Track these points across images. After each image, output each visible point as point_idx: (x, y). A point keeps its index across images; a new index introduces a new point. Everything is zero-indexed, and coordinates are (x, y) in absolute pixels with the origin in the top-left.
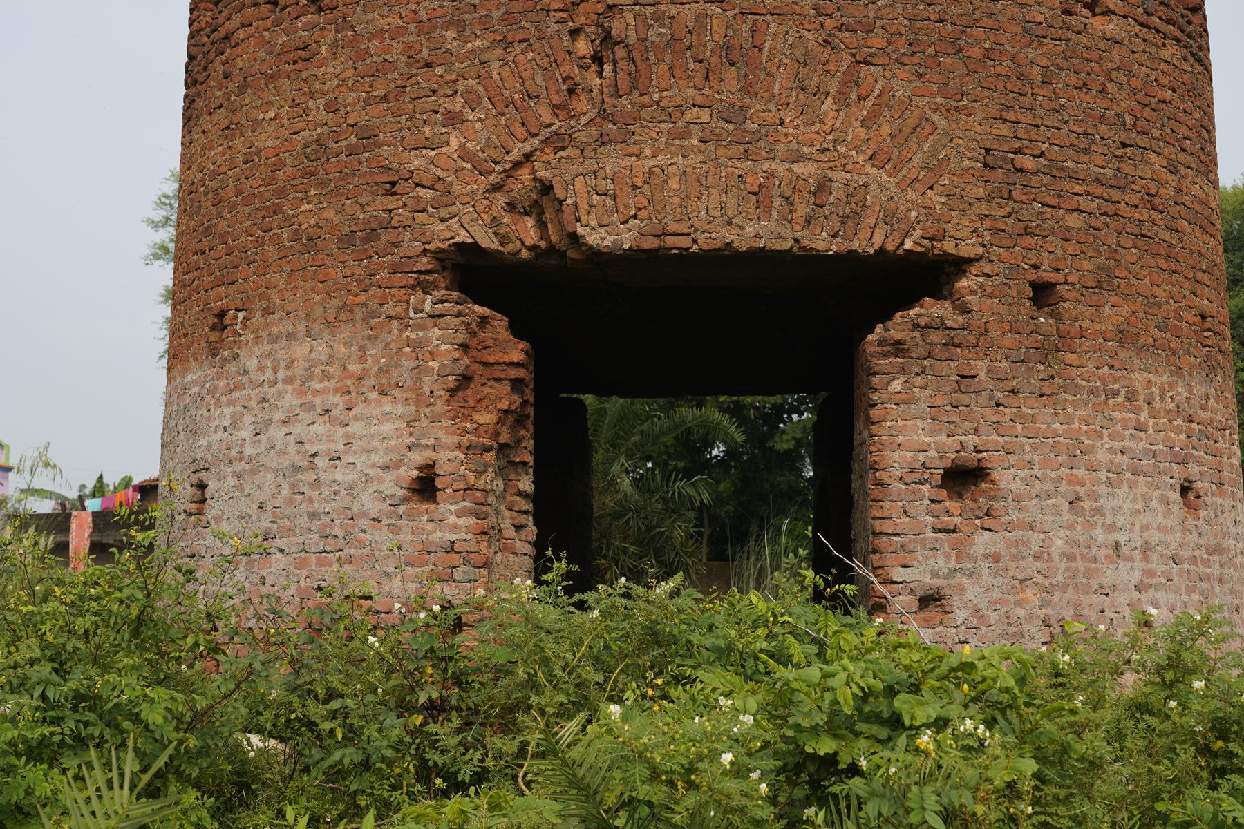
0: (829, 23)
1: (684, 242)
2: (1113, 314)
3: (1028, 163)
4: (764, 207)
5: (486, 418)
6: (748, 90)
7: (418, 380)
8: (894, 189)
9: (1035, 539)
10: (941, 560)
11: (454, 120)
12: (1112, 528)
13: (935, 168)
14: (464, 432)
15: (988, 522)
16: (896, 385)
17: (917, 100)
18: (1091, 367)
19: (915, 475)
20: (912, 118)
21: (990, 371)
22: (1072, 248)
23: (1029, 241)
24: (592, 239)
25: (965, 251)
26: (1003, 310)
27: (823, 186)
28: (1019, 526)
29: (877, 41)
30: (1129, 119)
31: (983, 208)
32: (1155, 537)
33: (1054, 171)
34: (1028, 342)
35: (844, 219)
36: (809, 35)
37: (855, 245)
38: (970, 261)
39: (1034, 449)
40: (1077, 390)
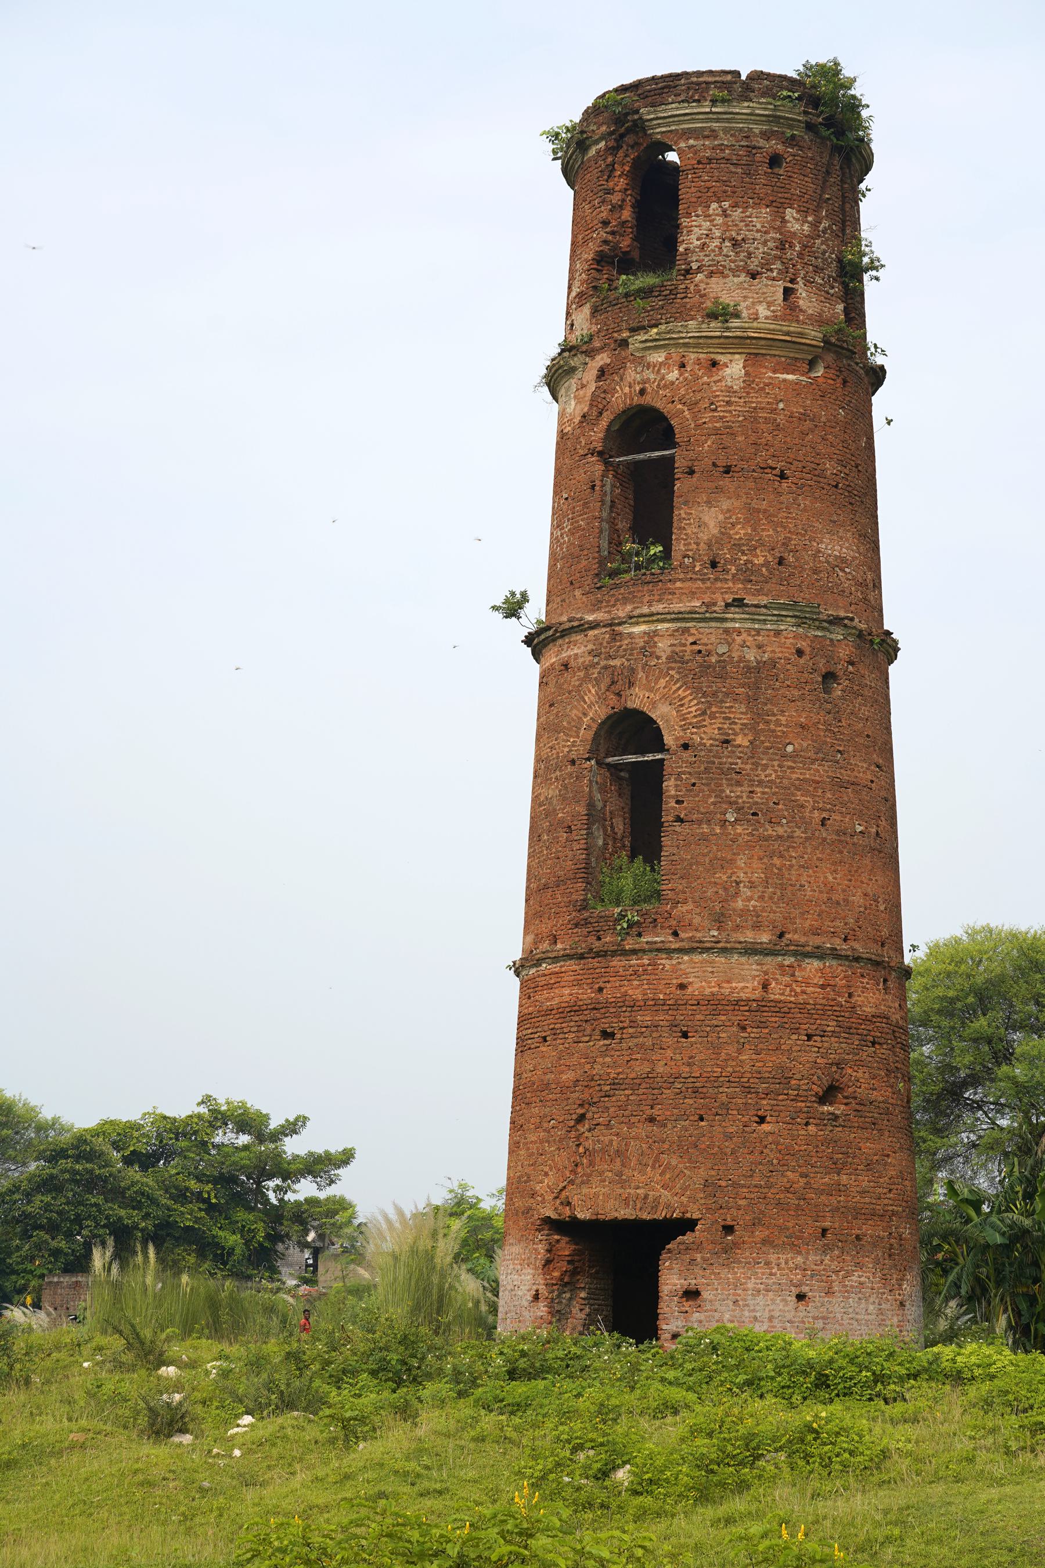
0: (650, 1140)
1: (603, 1217)
2: (760, 1234)
3: (723, 1183)
4: (627, 1205)
5: (556, 1274)
6: (623, 1165)
7: (535, 1261)
8: (669, 1197)
9: (717, 1315)
10: (679, 1322)
11: (546, 1174)
12: (754, 1311)
13: (685, 1189)
14: (546, 1279)
15: (699, 1309)
16: (667, 1264)
17: (681, 1166)
18: (747, 1254)
19: (672, 1294)
20: (677, 1171)
21: (702, 1258)
22: (741, 1212)
23: (722, 1211)
24: (579, 1216)
25: (694, 1217)
26: (709, 1236)
27: (646, 1197)
28: (711, 1310)
29: (666, 1146)
30: (775, 1161)
31: (703, 1201)
32: (777, 1314)
33: (735, 1185)
34: (719, 1247)
35: (652, 1208)
36: (644, 1145)
37: (655, 1217)
38: (698, 1220)
39: (719, 1284)
40: (741, 1262)
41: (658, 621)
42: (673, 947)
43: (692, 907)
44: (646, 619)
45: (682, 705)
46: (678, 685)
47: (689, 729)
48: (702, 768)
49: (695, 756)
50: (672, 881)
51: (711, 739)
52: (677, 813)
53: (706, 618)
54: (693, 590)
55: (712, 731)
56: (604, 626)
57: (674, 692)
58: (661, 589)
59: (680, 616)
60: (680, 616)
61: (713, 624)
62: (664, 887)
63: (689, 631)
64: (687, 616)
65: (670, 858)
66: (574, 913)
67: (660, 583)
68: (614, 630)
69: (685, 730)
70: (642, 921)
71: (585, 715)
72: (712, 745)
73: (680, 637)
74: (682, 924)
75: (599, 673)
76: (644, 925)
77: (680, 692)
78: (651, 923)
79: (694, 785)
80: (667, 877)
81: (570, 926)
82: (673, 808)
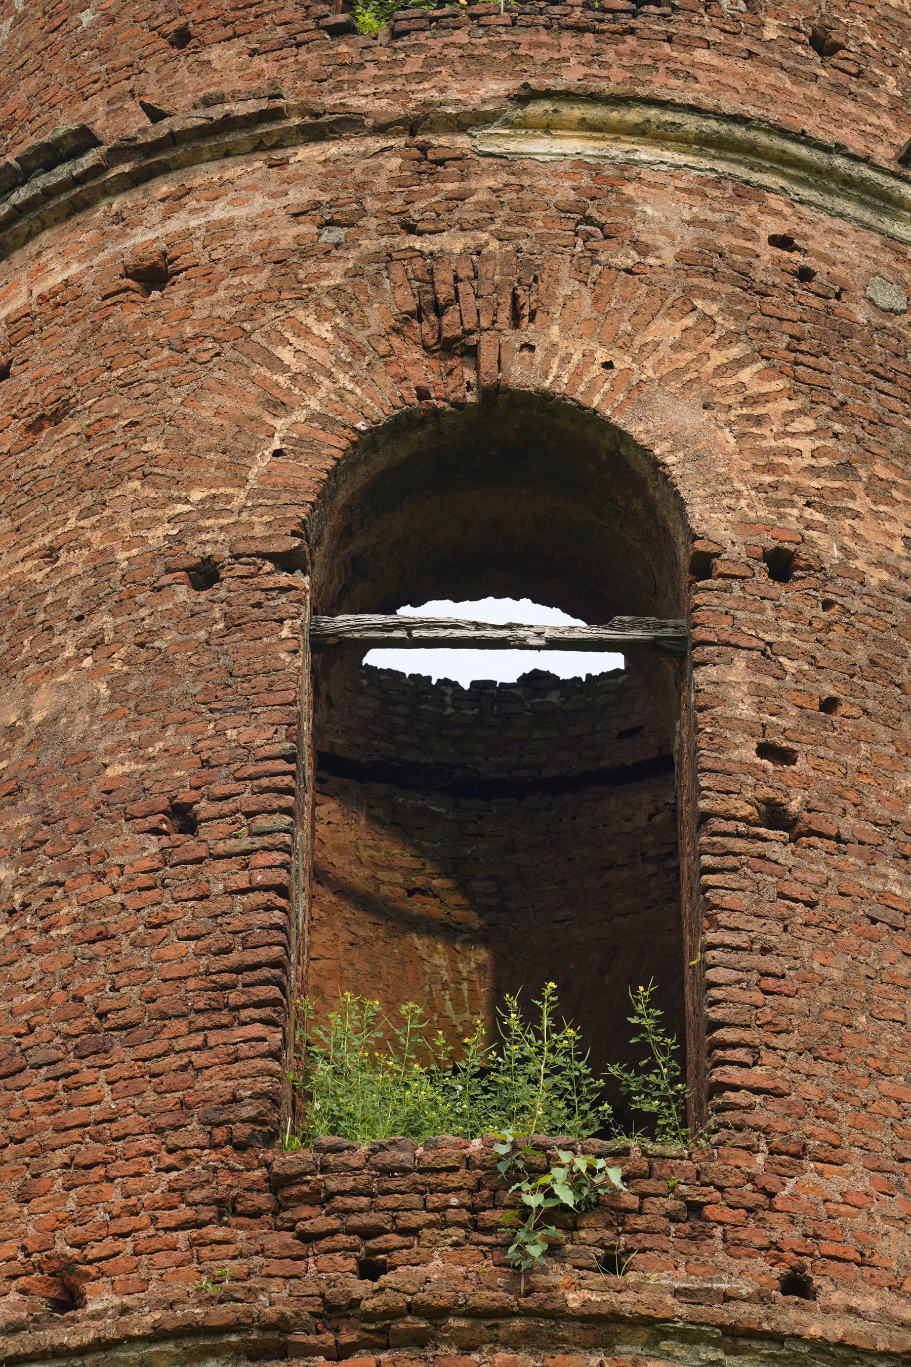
41: (640, 131)
42: (815, 1330)
43: (864, 1185)
44: (595, 113)
45: (759, 421)
46: (735, 351)
47: (792, 504)
48: (861, 655)
49: (827, 605)
50: (768, 1057)
51: (879, 564)
52: (766, 792)
53: (831, 173)
54: (762, 88)
55: (882, 539)
56: (381, 129)
57: (720, 371)
58: (633, 53)
59: (739, 132)
60: (739, 132)
61: (850, 208)
62: (734, 1075)
63: (761, 201)
64: (763, 139)
65: (747, 960)
66: (210, 1157)
67: (629, 39)
68: (424, 148)
69: (779, 504)
70: (631, 1201)
71: (278, 406)
72: (886, 588)
73: (726, 206)
74: (829, 1248)
75: (355, 274)
76: (640, 1222)
77: (745, 375)
78: (673, 1218)
79: (829, 705)
80: (746, 1036)
81: (184, 1213)
82: (750, 769)
